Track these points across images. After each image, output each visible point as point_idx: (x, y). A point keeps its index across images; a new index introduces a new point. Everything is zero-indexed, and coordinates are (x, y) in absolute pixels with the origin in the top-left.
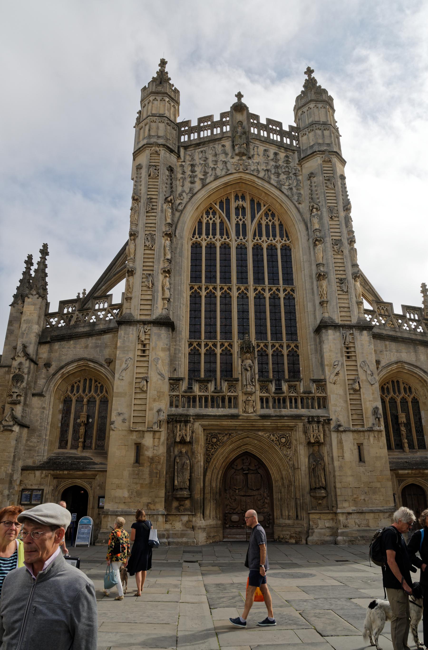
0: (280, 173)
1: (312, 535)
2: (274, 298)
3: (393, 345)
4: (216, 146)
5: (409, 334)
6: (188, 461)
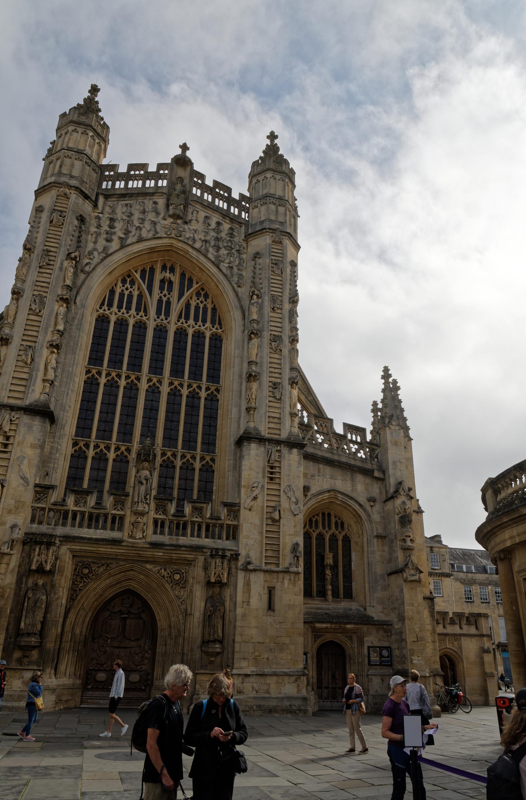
0: (221, 246)
2: (193, 397)
3: (327, 470)
4: (146, 202)
6: (44, 597)
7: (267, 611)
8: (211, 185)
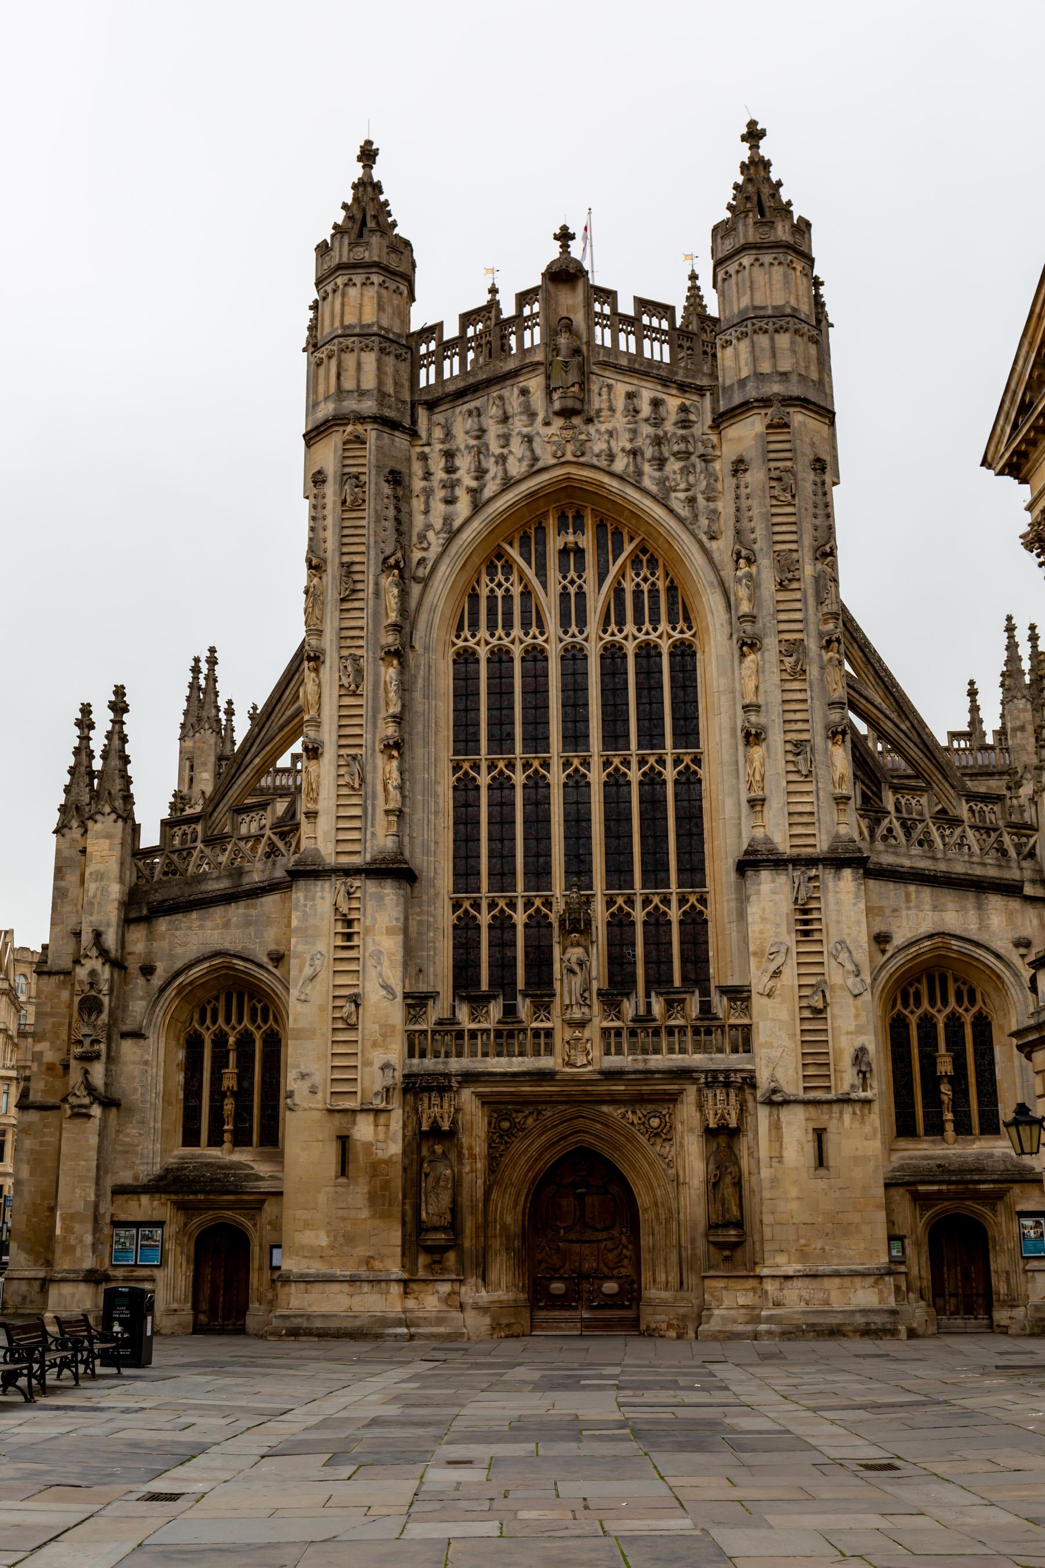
0: (667, 455)
1: (708, 1322)
2: (652, 781)
3: (926, 894)
5: (967, 865)
6: (448, 1172)
7: (816, 1169)
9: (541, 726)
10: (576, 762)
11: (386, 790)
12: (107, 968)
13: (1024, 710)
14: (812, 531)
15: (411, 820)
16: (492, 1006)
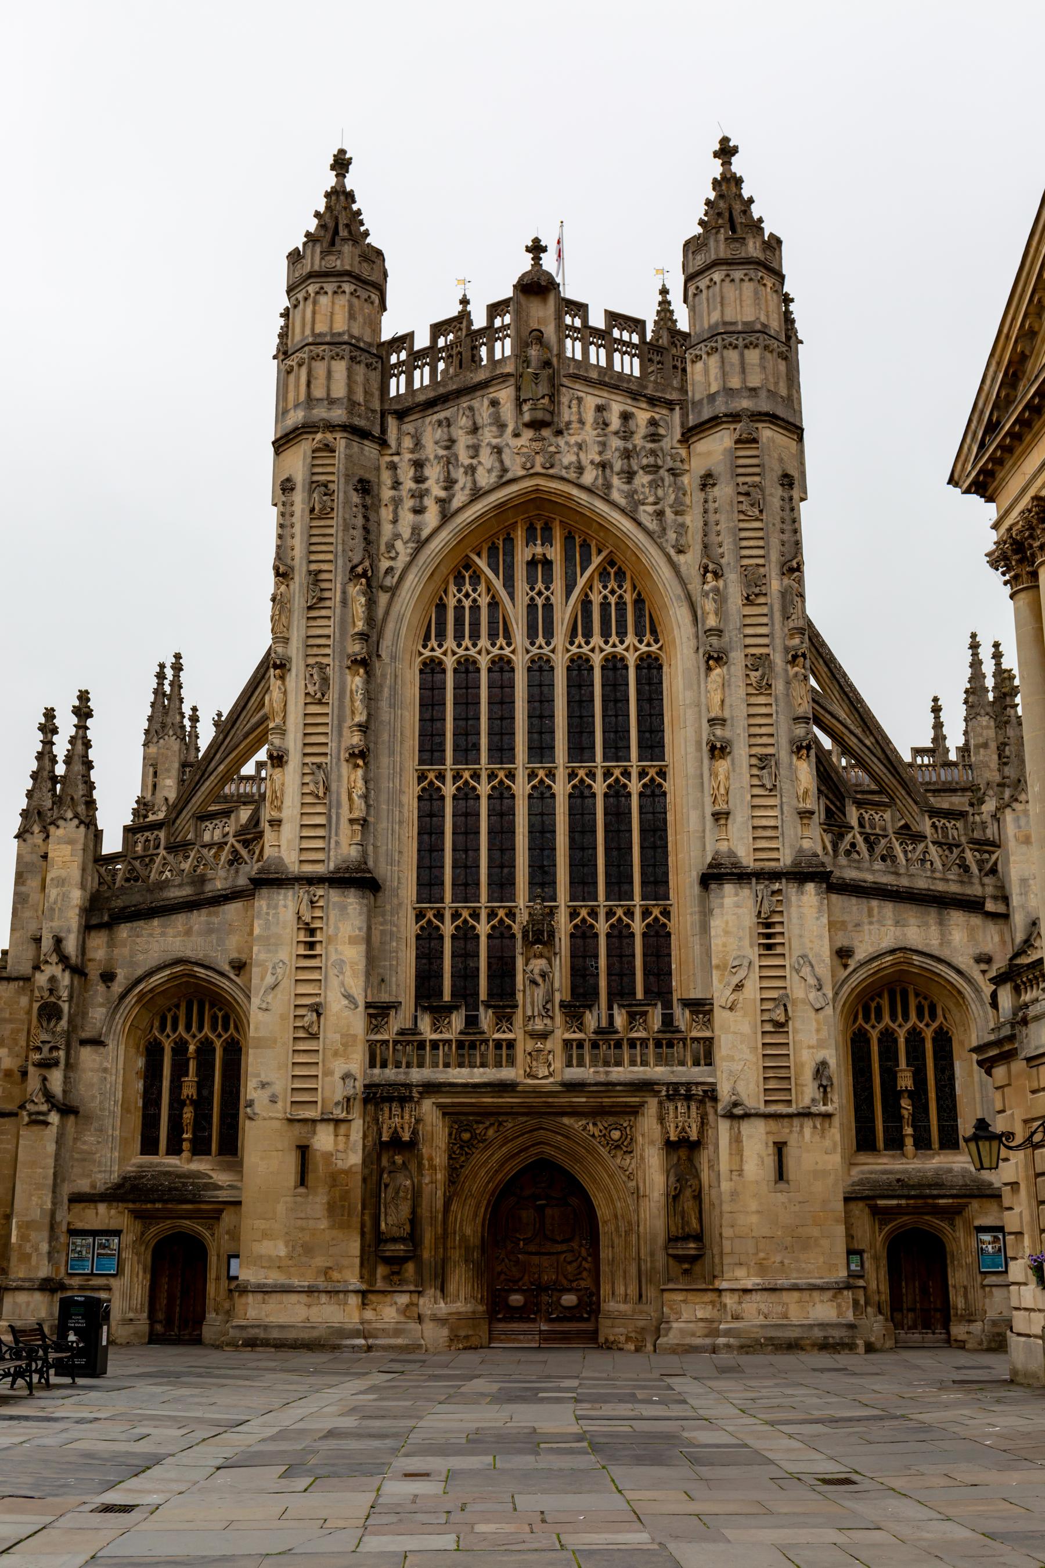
0: (635, 468)
1: (666, 1335)
2: (617, 793)
3: (888, 910)
5: (930, 880)
6: (408, 1183)
7: (776, 1183)
8: (601, 325)
9: (507, 737)
10: (541, 774)
11: (350, 799)
12: (67, 974)
13: (988, 727)
14: (779, 547)
15: (376, 830)
16: (454, 1016)
